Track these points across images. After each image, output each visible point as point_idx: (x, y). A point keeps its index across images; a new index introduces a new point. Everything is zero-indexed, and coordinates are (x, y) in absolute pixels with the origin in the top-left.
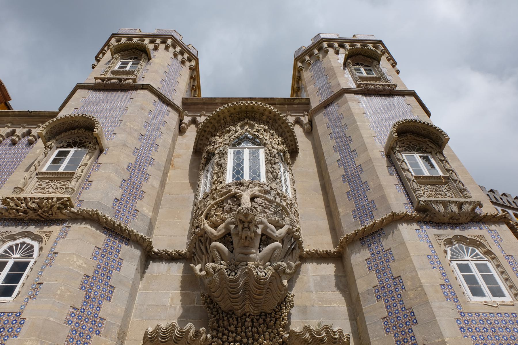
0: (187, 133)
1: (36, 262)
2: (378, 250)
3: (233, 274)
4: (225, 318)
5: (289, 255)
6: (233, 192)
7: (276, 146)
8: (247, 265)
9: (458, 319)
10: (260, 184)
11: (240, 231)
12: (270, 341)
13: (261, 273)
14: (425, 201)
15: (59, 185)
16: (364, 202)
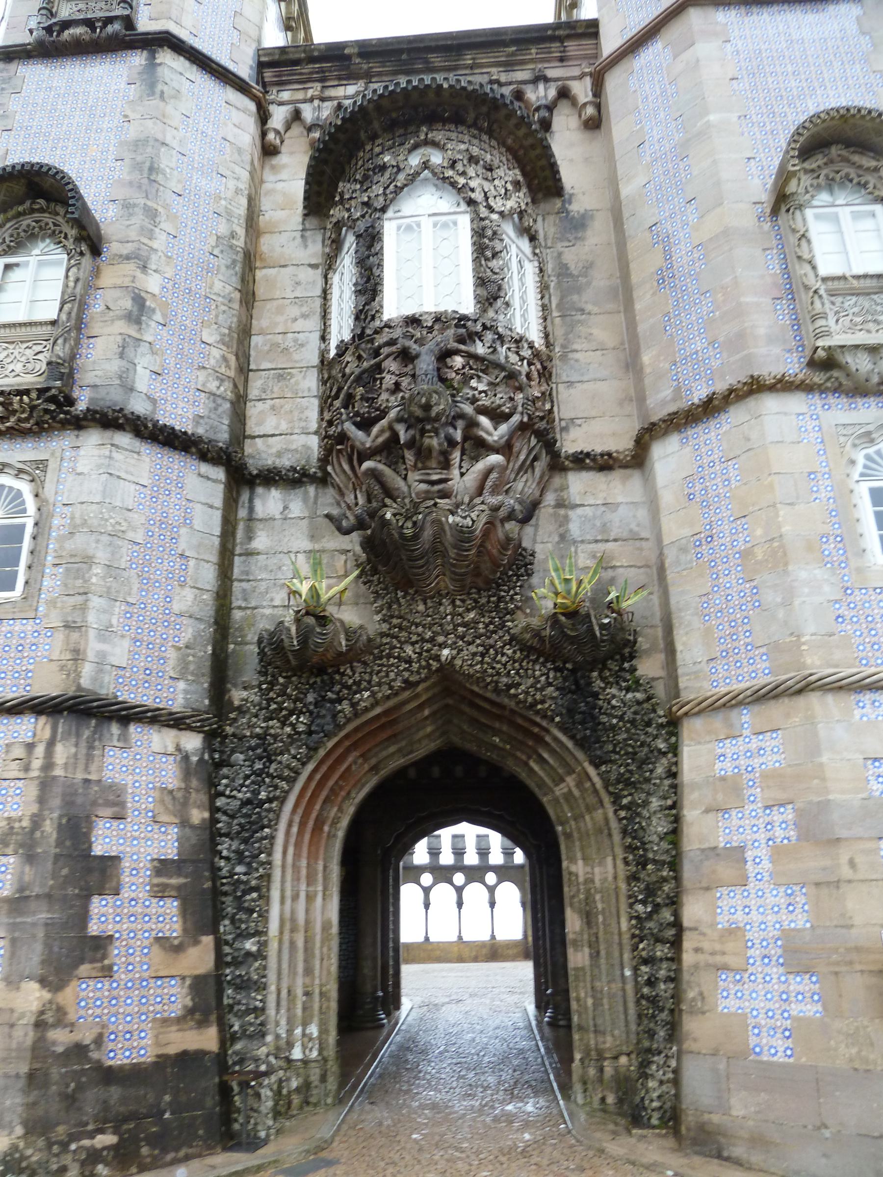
0: (283, 159)
1: (36, 524)
2: (711, 458)
3: (409, 524)
4: (402, 601)
5: (526, 472)
6: (399, 346)
7: (497, 204)
8: (435, 504)
9: (836, 602)
10: (460, 319)
11: (418, 437)
12: (489, 638)
13: (465, 518)
14: (830, 347)
15: (28, 351)
16: (699, 344)
